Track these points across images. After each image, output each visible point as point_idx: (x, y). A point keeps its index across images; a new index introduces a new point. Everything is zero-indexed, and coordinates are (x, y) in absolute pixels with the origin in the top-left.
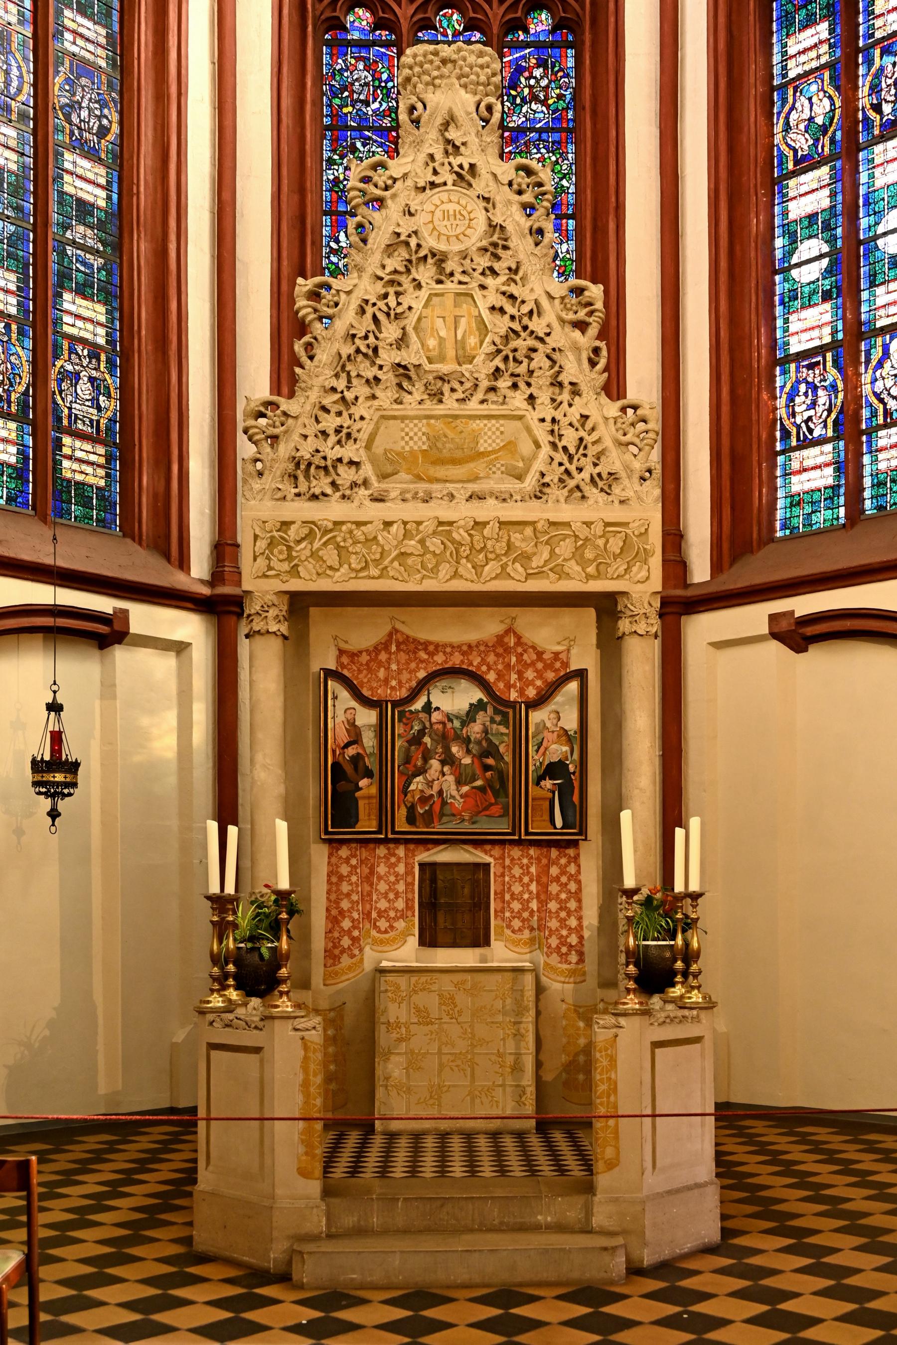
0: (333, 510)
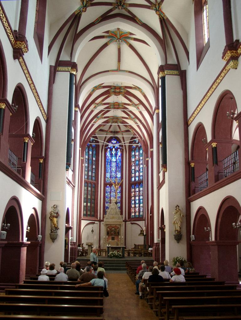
0: (108, 220)
